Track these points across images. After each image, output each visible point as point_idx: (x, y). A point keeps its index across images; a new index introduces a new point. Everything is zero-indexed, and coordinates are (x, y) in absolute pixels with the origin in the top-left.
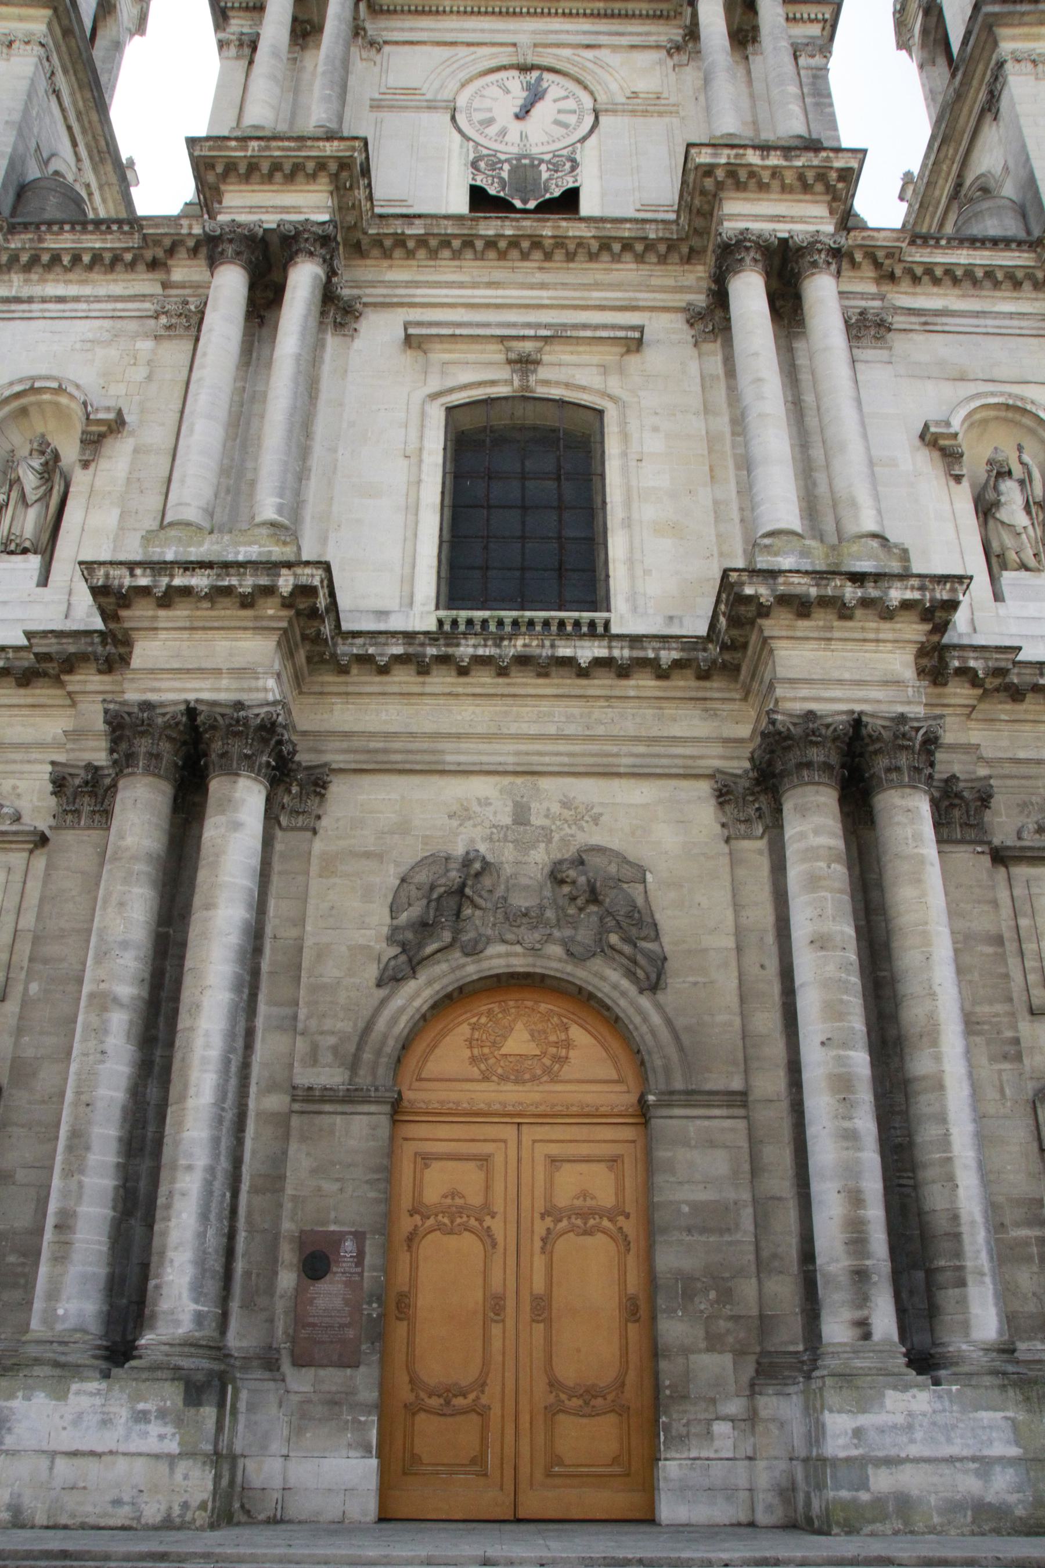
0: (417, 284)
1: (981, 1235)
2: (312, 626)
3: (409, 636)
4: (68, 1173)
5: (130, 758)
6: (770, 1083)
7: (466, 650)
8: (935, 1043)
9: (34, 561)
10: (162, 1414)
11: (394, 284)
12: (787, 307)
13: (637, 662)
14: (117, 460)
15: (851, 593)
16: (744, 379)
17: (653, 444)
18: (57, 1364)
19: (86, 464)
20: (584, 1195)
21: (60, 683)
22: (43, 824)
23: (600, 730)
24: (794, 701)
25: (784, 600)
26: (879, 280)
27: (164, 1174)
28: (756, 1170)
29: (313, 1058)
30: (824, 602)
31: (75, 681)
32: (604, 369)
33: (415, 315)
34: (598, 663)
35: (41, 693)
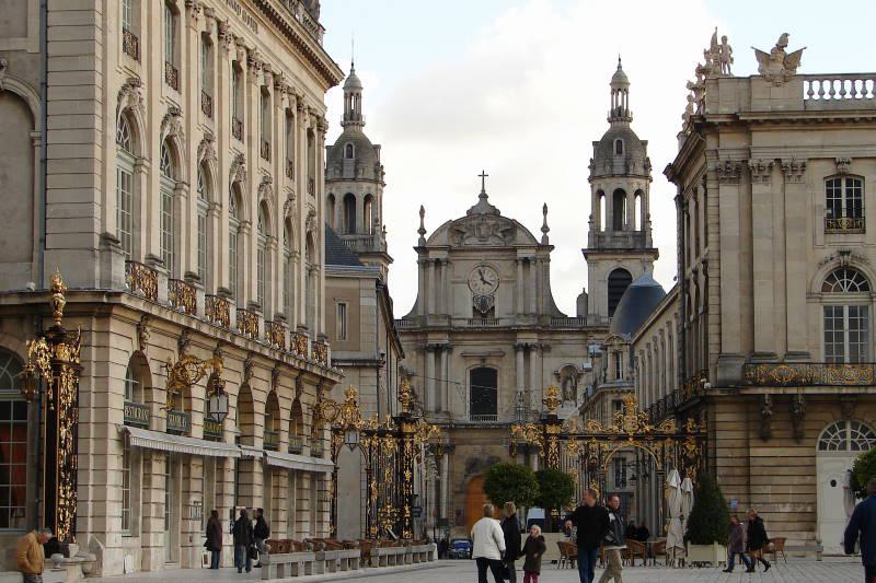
3: (466, 425)
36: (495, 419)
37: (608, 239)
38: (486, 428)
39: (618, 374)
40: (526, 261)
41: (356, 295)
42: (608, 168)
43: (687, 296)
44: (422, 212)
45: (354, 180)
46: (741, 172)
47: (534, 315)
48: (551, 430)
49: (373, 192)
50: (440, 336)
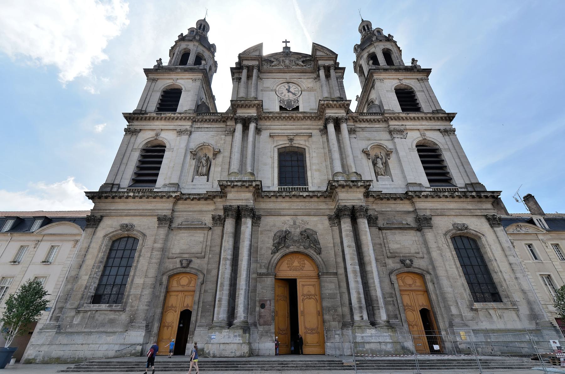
0: (271, 125)
1: (382, 300)
2: (259, 192)
3: (274, 192)
4: (220, 291)
5: (228, 215)
6: (341, 271)
7: (284, 194)
8: (371, 265)
9: (206, 177)
10: (239, 335)
11: (268, 125)
12: (338, 129)
13: (314, 195)
14: (220, 158)
15: (351, 184)
16: (331, 144)
17: (314, 155)
18: (220, 327)
19: (214, 159)
20: (309, 292)
21: (212, 200)
22: (210, 226)
23: (308, 208)
24: (343, 203)
25: (340, 185)
27: (237, 290)
28: (339, 287)
29: (261, 267)
30: (347, 185)
31: (215, 200)
32: (305, 141)
34: (307, 196)
35: (209, 202)
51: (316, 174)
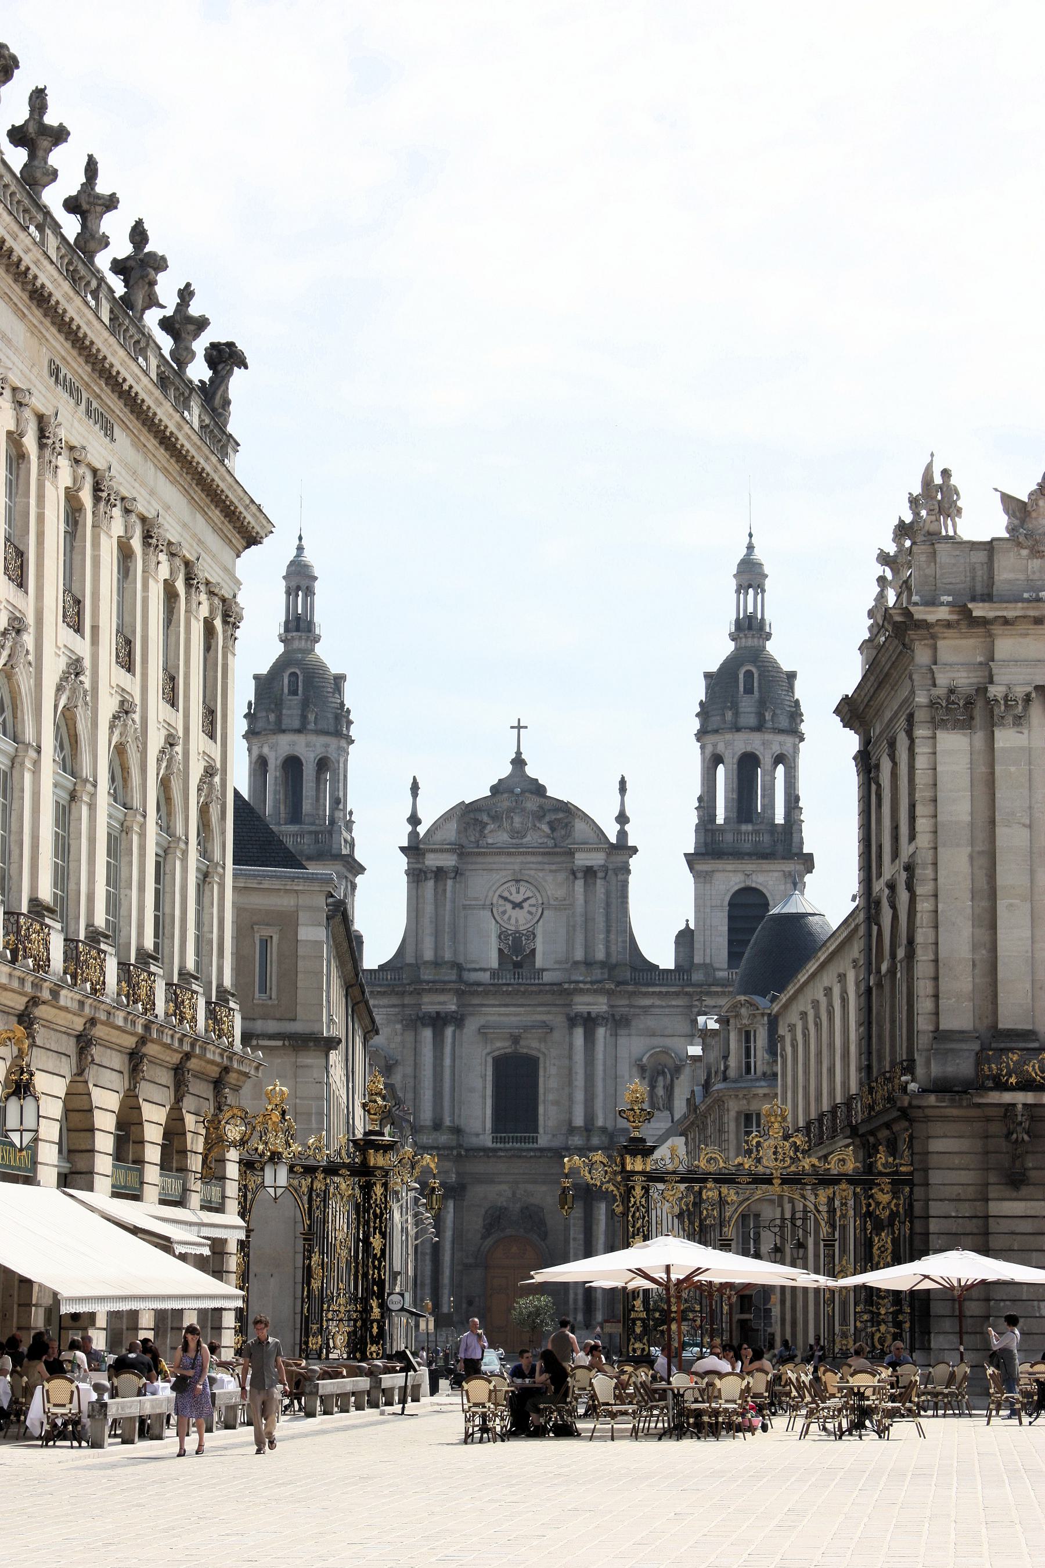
17: (553, 1071)
26: (629, 998)
33: (480, 1021)
36: (535, 1140)
37: (729, 837)
38: (517, 1155)
39: (748, 1065)
40: (589, 872)
41: (288, 922)
42: (729, 715)
43: (875, 928)
44: (415, 788)
45: (299, 731)
46: (975, 709)
47: (603, 964)
48: (635, 1164)
49: (332, 755)
50: (442, 998)
51: (553, 1110)
